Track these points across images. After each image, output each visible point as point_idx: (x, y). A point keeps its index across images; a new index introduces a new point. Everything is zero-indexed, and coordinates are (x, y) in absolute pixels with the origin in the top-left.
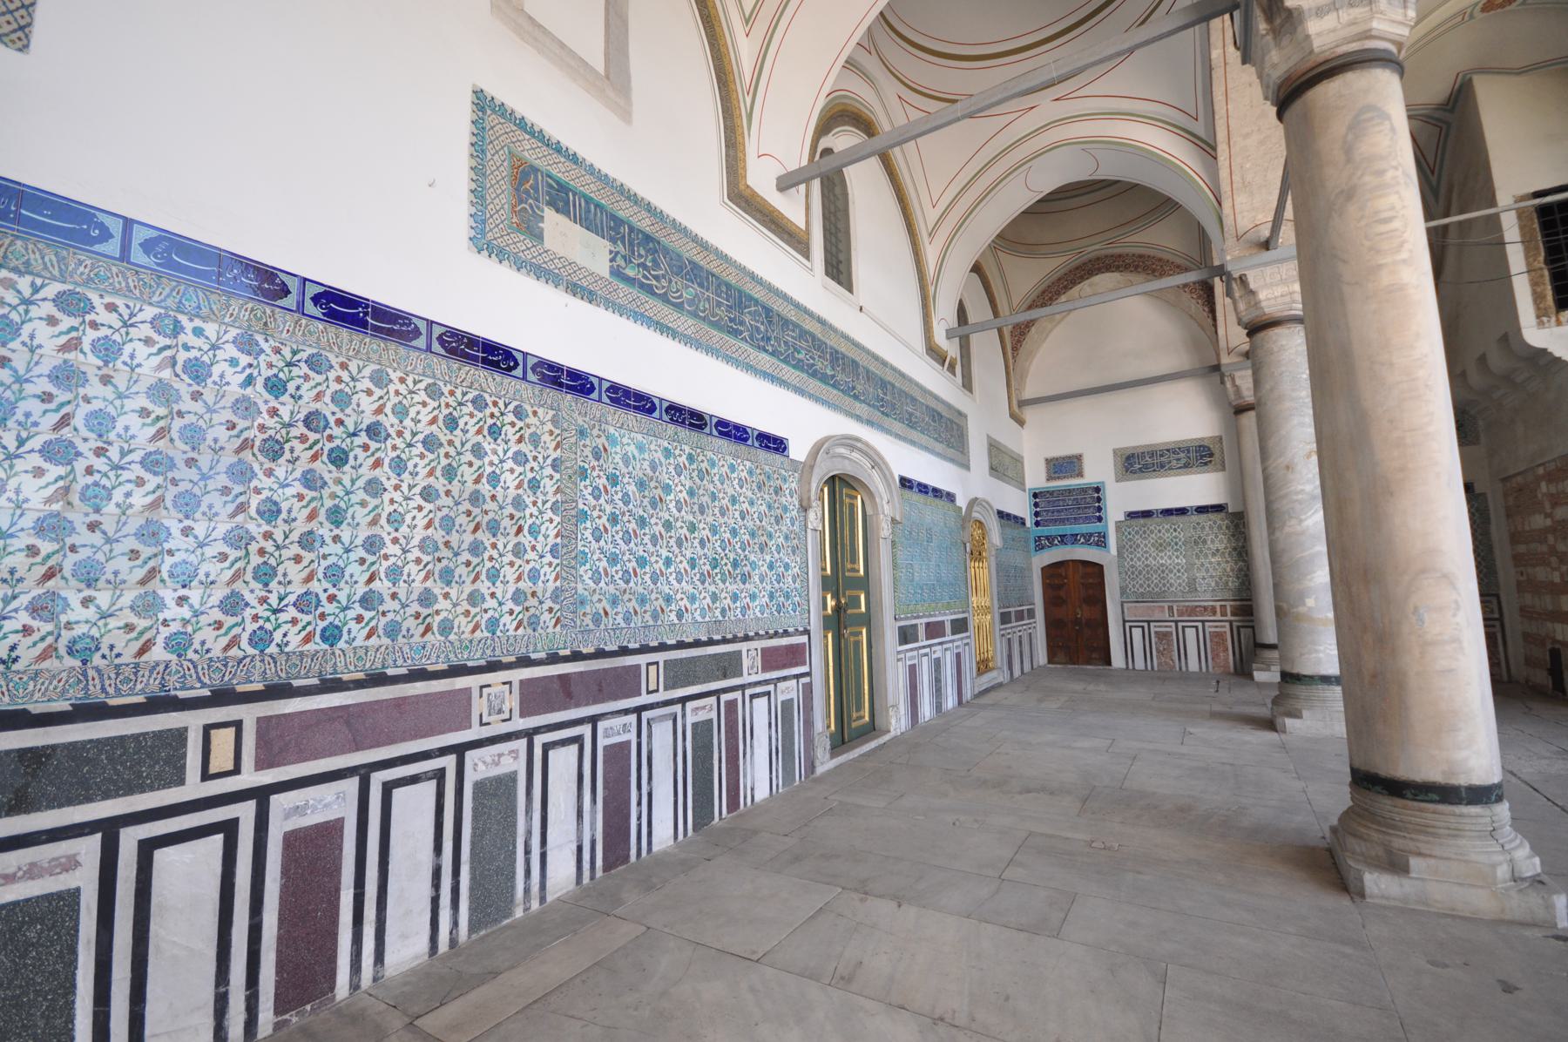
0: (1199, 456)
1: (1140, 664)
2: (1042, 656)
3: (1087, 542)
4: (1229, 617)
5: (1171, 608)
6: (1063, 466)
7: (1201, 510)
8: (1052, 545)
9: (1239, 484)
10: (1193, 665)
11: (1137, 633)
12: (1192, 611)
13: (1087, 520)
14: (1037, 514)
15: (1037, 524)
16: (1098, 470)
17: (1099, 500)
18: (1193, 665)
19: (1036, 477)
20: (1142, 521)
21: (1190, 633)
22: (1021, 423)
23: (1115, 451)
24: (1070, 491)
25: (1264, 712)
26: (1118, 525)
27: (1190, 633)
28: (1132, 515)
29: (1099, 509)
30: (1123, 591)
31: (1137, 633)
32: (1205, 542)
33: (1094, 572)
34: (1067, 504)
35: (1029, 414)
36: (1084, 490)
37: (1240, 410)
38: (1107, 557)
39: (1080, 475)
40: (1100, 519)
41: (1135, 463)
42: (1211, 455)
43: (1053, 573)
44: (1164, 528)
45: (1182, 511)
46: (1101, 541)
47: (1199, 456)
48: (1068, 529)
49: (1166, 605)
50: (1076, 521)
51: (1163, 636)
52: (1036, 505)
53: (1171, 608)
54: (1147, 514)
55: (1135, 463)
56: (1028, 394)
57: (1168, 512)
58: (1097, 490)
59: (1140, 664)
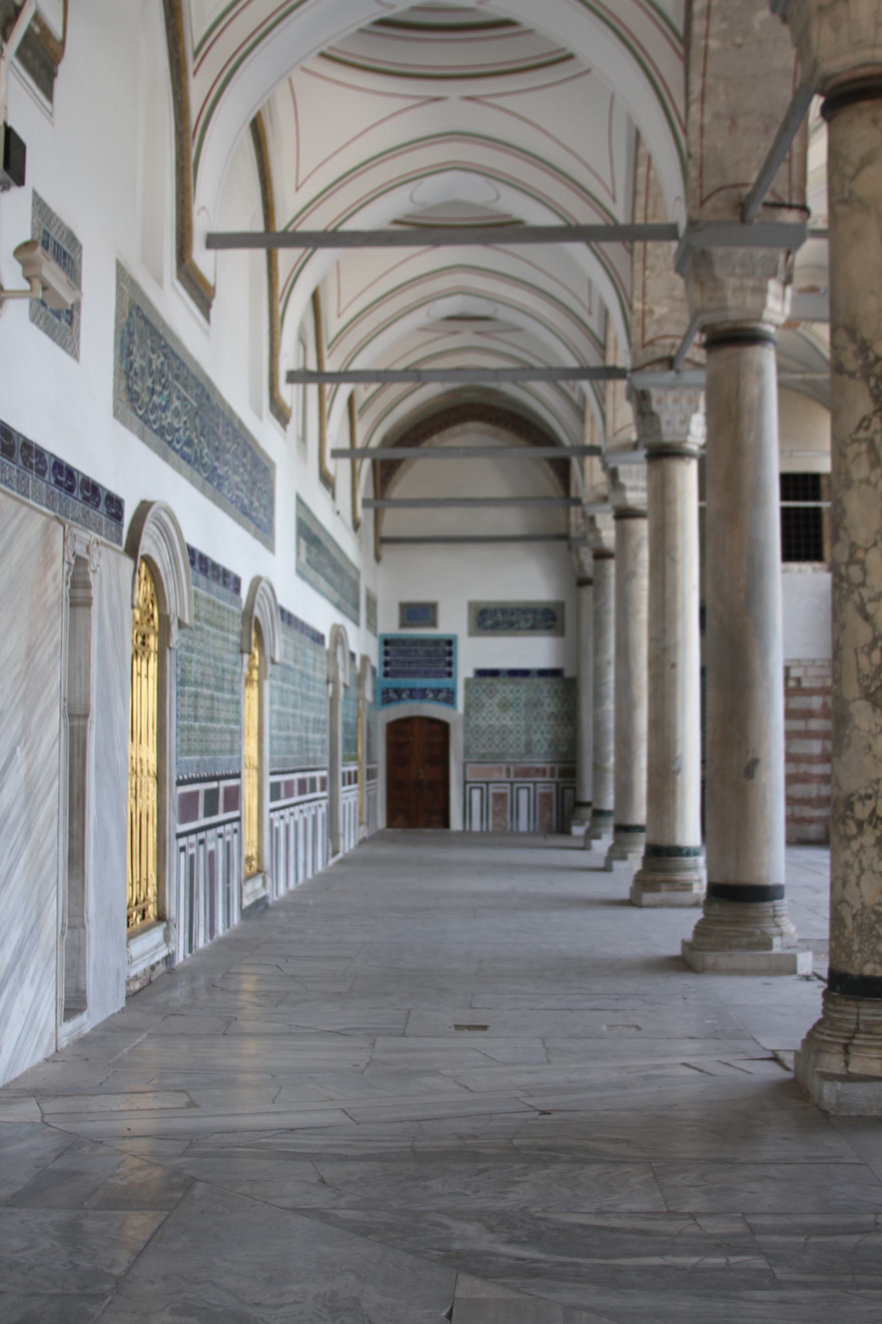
0: (545, 619)
1: (476, 826)
2: (381, 821)
3: (436, 699)
4: (556, 779)
5: (508, 770)
6: (418, 613)
7: (542, 673)
8: (400, 698)
9: (575, 652)
10: (523, 825)
11: (476, 794)
12: (525, 773)
13: (438, 674)
14: (386, 664)
15: (386, 674)
16: (453, 622)
17: (450, 654)
18: (523, 825)
19: (390, 623)
20: (488, 680)
21: (523, 794)
22: (378, 558)
23: (472, 606)
24: (423, 642)
25: (581, 844)
26: (468, 682)
27: (523, 794)
28: (481, 673)
29: (450, 664)
30: (467, 750)
31: (476, 794)
32: (542, 705)
33: (442, 728)
34: (414, 655)
35: (387, 552)
36: (436, 642)
37: (583, 582)
38: (454, 715)
39: (433, 624)
40: (450, 674)
41: (490, 619)
42: (554, 619)
43: (398, 731)
44: (506, 689)
45: (525, 673)
46: (449, 698)
47: (545, 619)
48: (419, 683)
49: (504, 767)
50: (426, 675)
51: (500, 798)
52: (386, 653)
53: (508, 770)
54: (494, 673)
55: (490, 619)
56: (387, 530)
57: (514, 673)
58: (450, 642)
59: (476, 826)
